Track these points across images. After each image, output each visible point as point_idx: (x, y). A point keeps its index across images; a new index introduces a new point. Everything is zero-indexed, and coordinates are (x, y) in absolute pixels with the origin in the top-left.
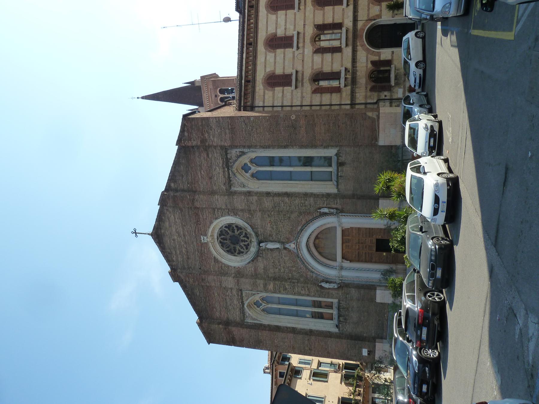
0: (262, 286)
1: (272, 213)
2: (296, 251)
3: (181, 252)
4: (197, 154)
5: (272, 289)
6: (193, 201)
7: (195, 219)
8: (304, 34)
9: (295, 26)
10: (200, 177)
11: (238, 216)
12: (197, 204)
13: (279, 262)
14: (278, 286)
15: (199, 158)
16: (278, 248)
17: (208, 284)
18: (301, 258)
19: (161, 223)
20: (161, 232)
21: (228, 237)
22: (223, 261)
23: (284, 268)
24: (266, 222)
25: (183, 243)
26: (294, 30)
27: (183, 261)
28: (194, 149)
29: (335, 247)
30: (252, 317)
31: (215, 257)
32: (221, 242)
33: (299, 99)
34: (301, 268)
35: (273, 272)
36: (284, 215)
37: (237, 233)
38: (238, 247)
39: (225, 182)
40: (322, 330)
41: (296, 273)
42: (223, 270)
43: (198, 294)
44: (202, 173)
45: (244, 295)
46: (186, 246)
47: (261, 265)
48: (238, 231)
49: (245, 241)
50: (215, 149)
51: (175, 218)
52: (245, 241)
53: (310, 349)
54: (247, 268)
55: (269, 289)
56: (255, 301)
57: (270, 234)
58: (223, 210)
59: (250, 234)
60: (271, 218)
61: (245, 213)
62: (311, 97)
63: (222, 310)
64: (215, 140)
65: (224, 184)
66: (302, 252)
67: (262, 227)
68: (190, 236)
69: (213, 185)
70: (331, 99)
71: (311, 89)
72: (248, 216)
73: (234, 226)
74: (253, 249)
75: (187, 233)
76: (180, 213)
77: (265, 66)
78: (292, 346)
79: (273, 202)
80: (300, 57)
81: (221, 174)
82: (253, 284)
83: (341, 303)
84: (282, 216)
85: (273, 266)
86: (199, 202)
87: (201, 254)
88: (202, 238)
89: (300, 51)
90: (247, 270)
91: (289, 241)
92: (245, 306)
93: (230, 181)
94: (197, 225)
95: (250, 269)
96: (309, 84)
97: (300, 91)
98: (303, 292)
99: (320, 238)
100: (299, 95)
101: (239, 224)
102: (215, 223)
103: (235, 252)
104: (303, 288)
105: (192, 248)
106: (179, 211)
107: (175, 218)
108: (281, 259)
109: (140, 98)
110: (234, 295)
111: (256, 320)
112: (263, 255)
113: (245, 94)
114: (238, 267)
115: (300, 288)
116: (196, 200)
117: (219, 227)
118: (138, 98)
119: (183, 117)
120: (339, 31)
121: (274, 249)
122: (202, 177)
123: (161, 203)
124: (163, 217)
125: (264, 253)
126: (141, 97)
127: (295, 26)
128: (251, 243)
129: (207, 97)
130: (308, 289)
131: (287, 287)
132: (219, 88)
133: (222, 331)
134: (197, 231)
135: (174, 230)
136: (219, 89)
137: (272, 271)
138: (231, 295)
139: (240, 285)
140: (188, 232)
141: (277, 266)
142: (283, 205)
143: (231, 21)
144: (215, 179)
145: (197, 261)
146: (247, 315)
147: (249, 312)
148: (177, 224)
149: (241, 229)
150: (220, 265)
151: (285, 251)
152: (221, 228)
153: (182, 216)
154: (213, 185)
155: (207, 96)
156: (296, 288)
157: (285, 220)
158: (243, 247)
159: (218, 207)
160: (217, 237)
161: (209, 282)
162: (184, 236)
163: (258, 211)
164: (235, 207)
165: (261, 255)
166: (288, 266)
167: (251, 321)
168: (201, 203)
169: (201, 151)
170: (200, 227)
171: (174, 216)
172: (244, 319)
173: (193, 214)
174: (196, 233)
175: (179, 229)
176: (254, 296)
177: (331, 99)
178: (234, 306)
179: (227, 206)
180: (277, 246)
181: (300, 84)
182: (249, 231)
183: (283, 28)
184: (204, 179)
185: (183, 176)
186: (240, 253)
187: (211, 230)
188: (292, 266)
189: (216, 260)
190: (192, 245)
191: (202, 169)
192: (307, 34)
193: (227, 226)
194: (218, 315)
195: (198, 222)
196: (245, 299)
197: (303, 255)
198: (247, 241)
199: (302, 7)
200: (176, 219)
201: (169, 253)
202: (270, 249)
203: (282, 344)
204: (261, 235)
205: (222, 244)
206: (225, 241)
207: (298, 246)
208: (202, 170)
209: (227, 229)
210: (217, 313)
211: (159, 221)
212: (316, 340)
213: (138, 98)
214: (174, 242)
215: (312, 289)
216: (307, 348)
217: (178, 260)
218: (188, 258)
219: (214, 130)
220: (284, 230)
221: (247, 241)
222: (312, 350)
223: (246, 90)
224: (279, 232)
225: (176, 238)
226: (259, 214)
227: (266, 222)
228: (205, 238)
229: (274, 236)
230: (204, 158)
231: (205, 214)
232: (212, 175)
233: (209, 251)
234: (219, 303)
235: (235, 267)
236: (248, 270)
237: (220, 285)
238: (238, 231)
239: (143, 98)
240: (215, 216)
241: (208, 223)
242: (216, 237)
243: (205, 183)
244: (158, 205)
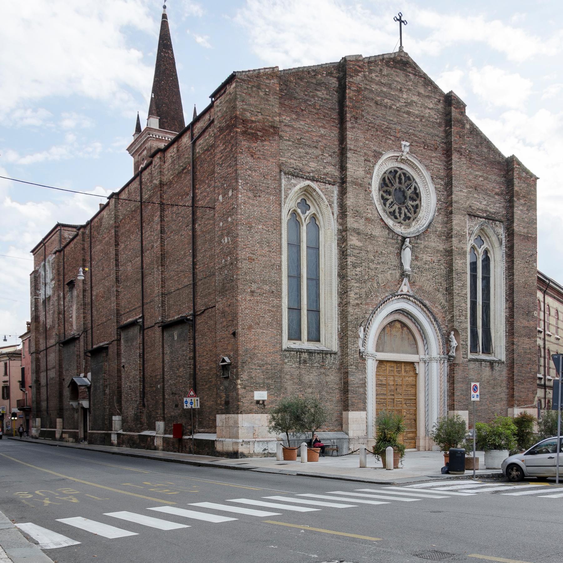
0: (355, 225)
1: (442, 267)
2: (399, 293)
3: (386, 95)
4: (498, 179)
5: (352, 243)
6: (459, 151)
7: (430, 144)
10: (477, 173)
11: (437, 214)
12: (455, 157)
13: (383, 262)
14: (358, 255)
15: (495, 180)
16: (402, 264)
17: (349, 125)
18: (389, 299)
19: (422, 80)
20: (410, 73)
21: (403, 187)
22: (377, 167)
23: (376, 269)
24: (432, 255)
25: (398, 105)
27: (371, 91)
28: (502, 177)
29: (392, 351)
31: (382, 154)
32: (396, 172)
34: (377, 296)
35: (368, 250)
36: (441, 283)
37: (410, 203)
38: (392, 200)
39: (473, 208)
41: (370, 287)
44: (481, 179)
45: (328, 186)
46: (394, 109)
47: (377, 231)
48: (413, 206)
49: (400, 213)
50: (503, 207)
51: (429, 109)
52: (400, 213)
53: (252, 292)
54: (371, 207)
55: (351, 237)
57: (418, 257)
58: (442, 193)
59: (409, 226)
60: (437, 264)
61: (441, 226)
63: (295, 132)
65: (470, 206)
66: (395, 301)
67: (426, 248)
68: (409, 124)
69: (469, 189)
72: (439, 229)
73: (417, 202)
74: (390, 222)
75: (412, 119)
76: (435, 121)
78: (254, 257)
79: (461, 271)
81: (479, 205)
82: (357, 212)
84: (440, 281)
85: (377, 252)
86: (458, 160)
87: (384, 132)
88: (408, 144)
90: (368, 205)
91: (412, 284)
92: (308, 182)
93: (475, 216)
94: (424, 142)
95: (369, 211)
98: (352, 295)
99: (402, 330)
101: (421, 211)
102: (427, 175)
103: (384, 191)
104: (358, 296)
105: (391, 119)
106: (438, 121)
107: (429, 109)
108: (388, 267)
110: (324, 168)
112: (391, 238)
114: (371, 191)
115: (358, 291)
116: (460, 157)
117: (415, 177)
119: (532, 175)
121: (401, 257)
122: (476, 176)
123: (455, 97)
124: (430, 89)
125: (393, 241)
128: (399, 223)
130: (358, 304)
131: (358, 269)
133: (268, 117)
134: (416, 138)
135: (415, 98)
137: (370, 248)
138: (325, 161)
139: (354, 186)
140: (413, 122)
141: (377, 258)
142: (459, 284)
144: (476, 196)
145: (374, 119)
146: (293, 181)
147: (298, 187)
148: (423, 109)
149: (415, 212)
150: (371, 159)
151: (398, 275)
152: (414, 180)
153: (434, 122)
154: (469, 189)
156: (357, 285)
157: (436, 283)
158: (392, 207)
159: (454, 189)
160: (402, 169)
162: (408, 113)
163: (444, 247)
164: (455, 215)
165: (391, 236)
166: (378, 276)
167: (283, 185)
168: (458, 164)
169: (501, 186)
170: (420, 147)
171: (432, 109)
173: (435, 142)
174: (412, 136)
175: (417, 108)
176: (329, 205)
178: (306, 159)
179: (455, 202)
180: (407, 267)
182: (413, 224)
184: (475, 178)
185: (477, 147)
186: (384, 200)
187: (416, 163)
188: (378, 283)
189: (377, 155)
190: (395, 120)
191: (484, 179)
193: (417, 192)
194: (285, 119)
195: (426, 145)
196: (322, 186)
197: (391, 303)
198: (400, 216)
200: (429, 111)
202: (400, 254)
203: (257, 237)
204: (417, 243)
205: (393, 173)
206: (397, 180)
207: (405, 296)
209: (413, 188)
210: (289, 119)
211: (425, 78)
212: (273, 307)
214: (398, 89)
215: (360, 310)
216: (254, 286)
217: (371, 82)
218: (376, 103)
219: (527, 214)
220: (424, 280)
221: (400, 216)
222: (253, 295)
224: (422, 272)
225: (405, 96)
226: (441, 247)
227: (432, 255)
228: (407, 149)
229: (416, 263)
230: (495, 188)
231: (437, 162)
232: (479, 193)
233: (390, 148)
234: (308, 132)
235: (370, 184)
236: (368, 207)
237: (350, 149)
238: (413, 206)
240: (436, 178)
241: (427, 162)
242: (402, 166)
243: (471, 177)
244: (451, 92)
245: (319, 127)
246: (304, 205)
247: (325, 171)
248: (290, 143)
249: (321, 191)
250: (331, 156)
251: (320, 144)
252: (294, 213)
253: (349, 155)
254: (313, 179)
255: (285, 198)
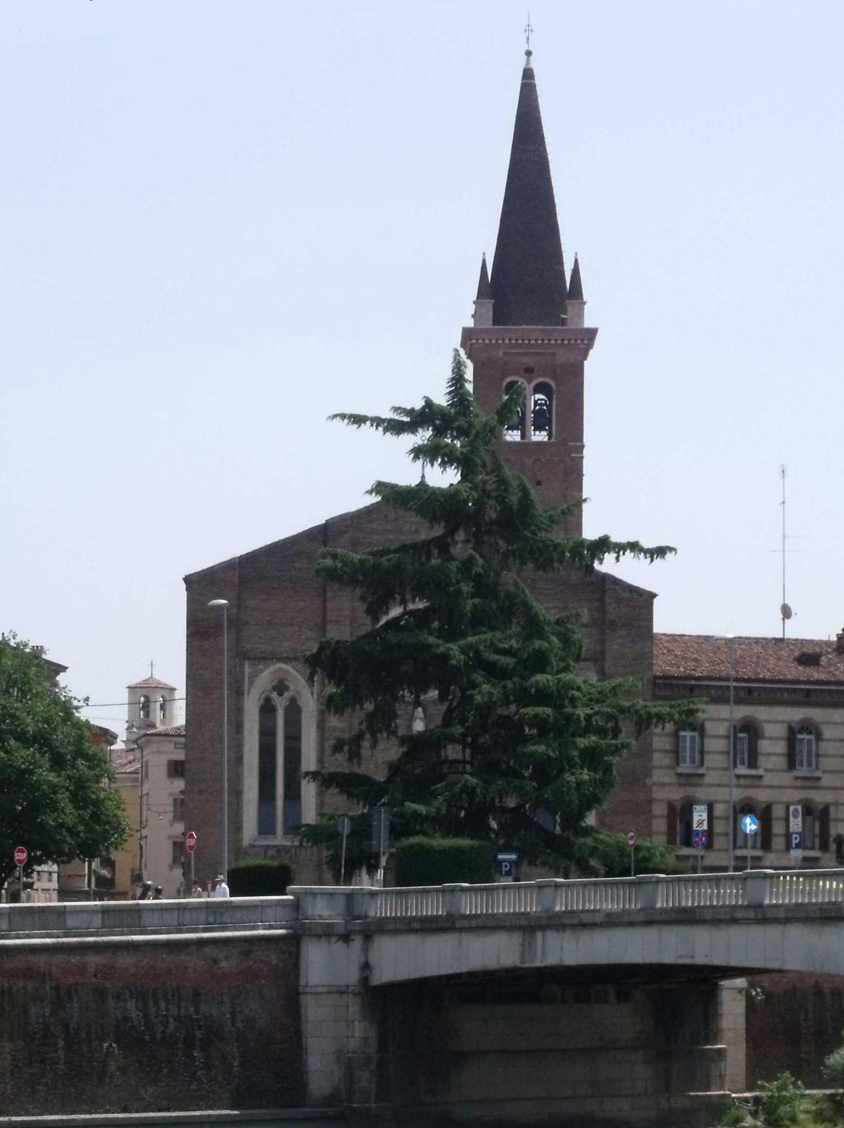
8: (759, 787)
9: (772, 770)
17: (329, 595)
26: (766, 770)
30: (256, 676)
33: (662, 780)
40: (244, 815)
42: (358, 627)
43: (297, 565)
56: (286, 683)
62: (662, 800)
64: (615, 647)
70: (658, 833)
71: (675, 800)
77: (712, 720)
80: (725, 780)
83: (306, 851)
89: (734, 781)
96: (681, 796)
97: (672, 781)
100: (667, 780)
109: (528, 62)
110: (302, 644)
111: (251, 683)
113: (671, 686)
118: (529, 53)
120: (759, 845)
126: (534, 65)
127: (772, 770)
129: (529, 340)
132: (558, 385)
136: (553, 384)
138: (303, 637)
143: (783, 620)
147: (266, 673)
155: (533, 342)
161: (334, 597)
172: (250, 659)
177: (658, 833)
181: (682, 781)
183: (770, 751)
192: (757, 790)
199: (799, 783)
201: (386, 516)
208: (556, 611)
213: (529, 53)
223: (678, 686)
239: (528, 74)
245: (296, 601)
246: (280, 687)
247: (303, 648)
248: (259, 627)
249: (298, 671)
250: (311, 630)
251: (297, 620)
252: (268, 700)
253: (329, 628)
254: (287, 660)
255: (249, 688)
